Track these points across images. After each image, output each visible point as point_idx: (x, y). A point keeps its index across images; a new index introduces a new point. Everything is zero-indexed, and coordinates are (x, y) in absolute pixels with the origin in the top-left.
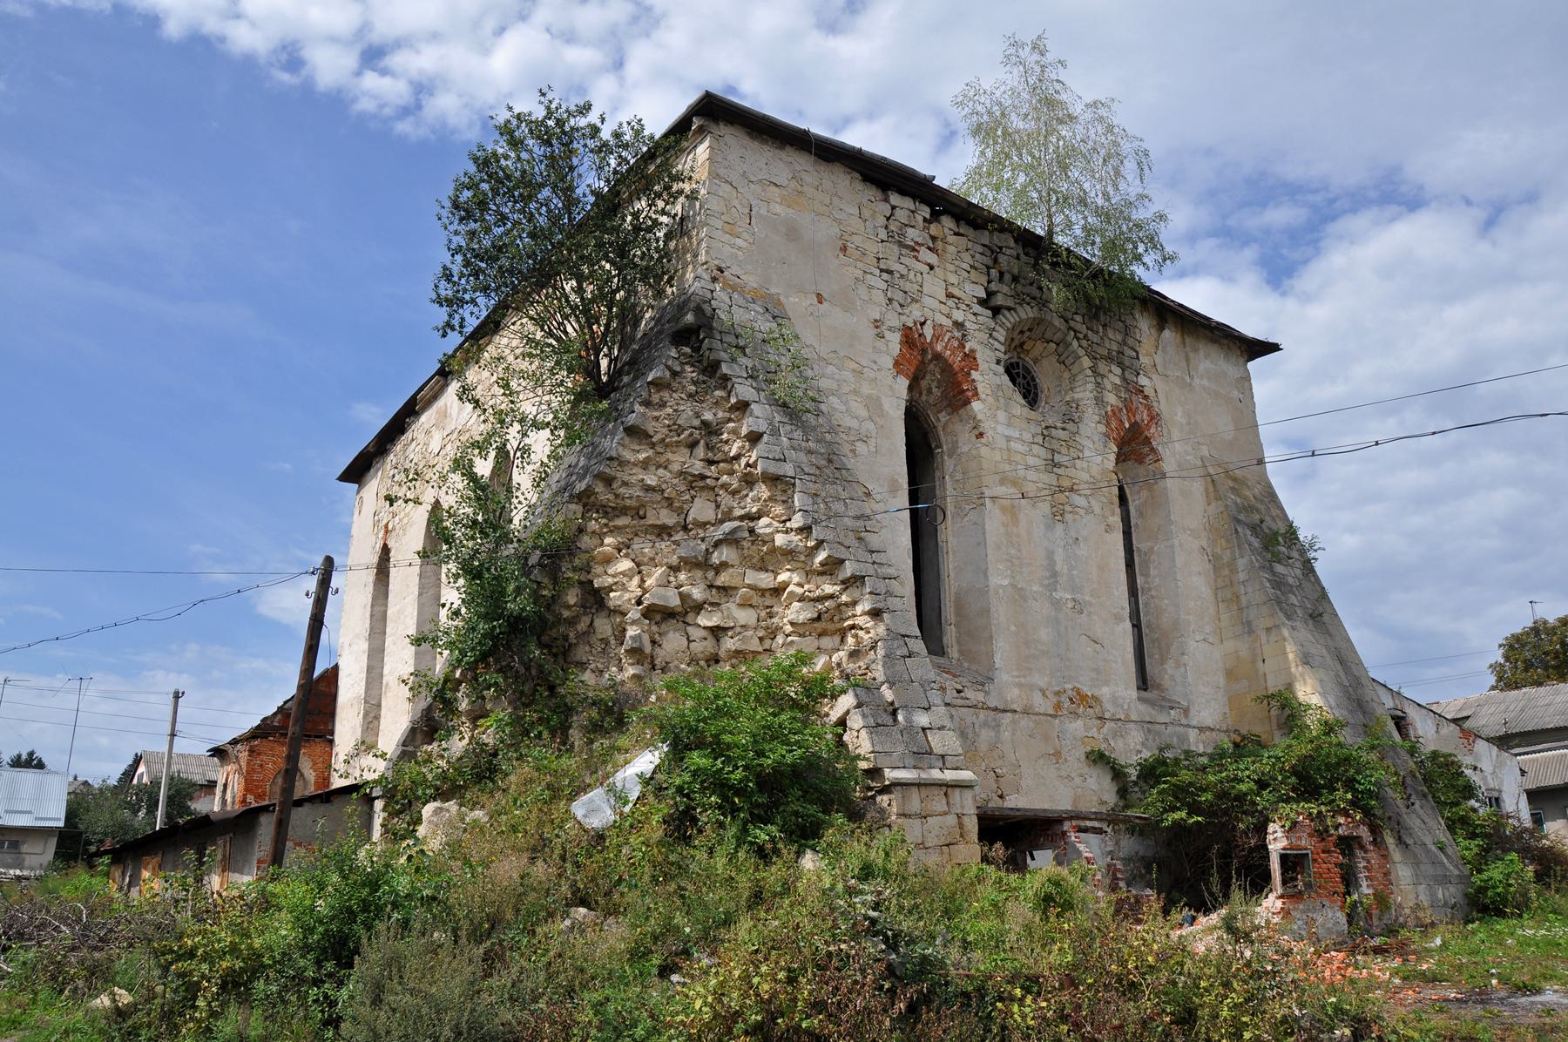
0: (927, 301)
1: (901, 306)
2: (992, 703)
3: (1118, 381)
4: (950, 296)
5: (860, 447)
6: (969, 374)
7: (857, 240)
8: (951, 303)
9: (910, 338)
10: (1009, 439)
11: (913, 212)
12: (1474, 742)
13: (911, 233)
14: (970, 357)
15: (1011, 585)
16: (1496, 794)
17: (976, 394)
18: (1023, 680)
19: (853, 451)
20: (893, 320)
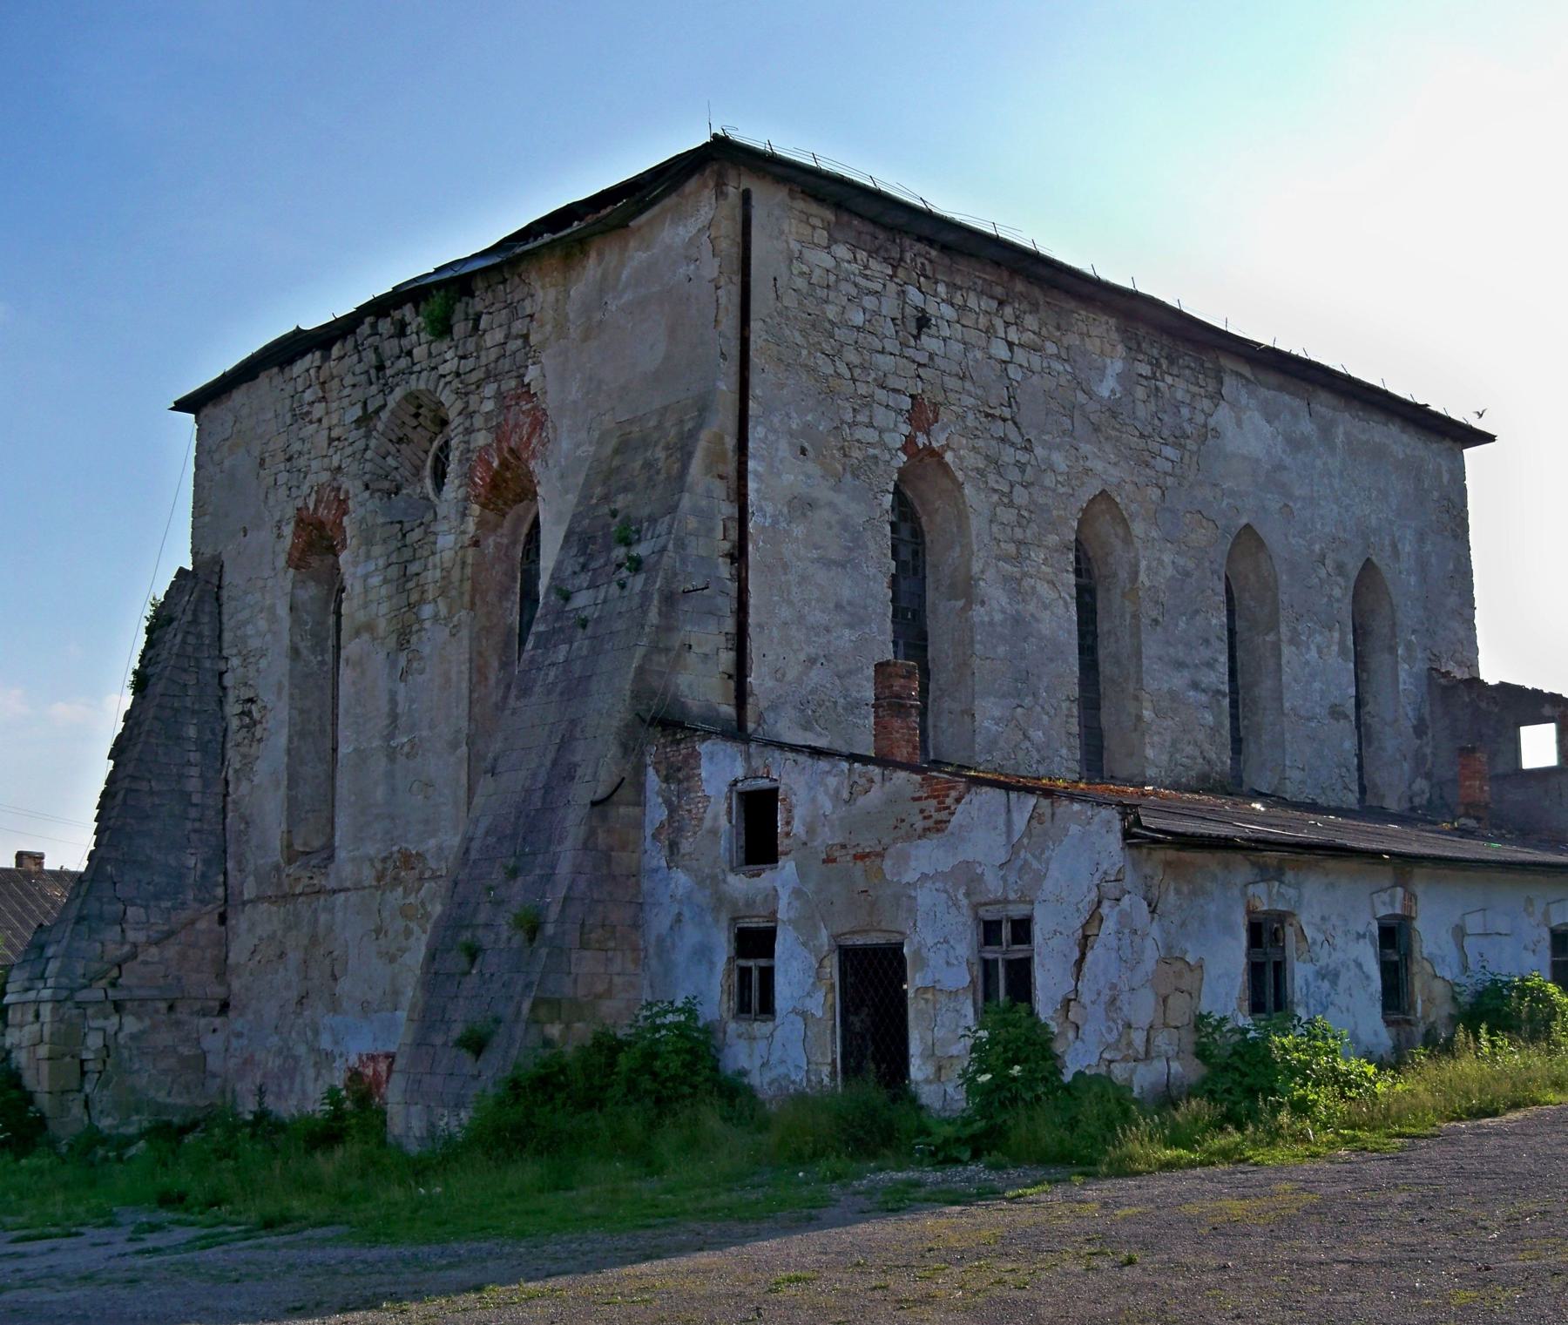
0: (315, 465)
1: (298, 487)
2: (331, 883)
3: (489, 406)
4: (331, 440)
5: (263, 663)
6: (341, 522)
7: (271, 447)
8: (332, 450)
9: (300, 522)
10: (366, 577)
11: (308, 370)
12: (958, 801)
13: (308, 396)
14: (342, 507)
15: (355, 749)
16: (1017, 911)
17: (344, 547)
18: (357, 853)
19: (258, 671)
20: (290, 512)
